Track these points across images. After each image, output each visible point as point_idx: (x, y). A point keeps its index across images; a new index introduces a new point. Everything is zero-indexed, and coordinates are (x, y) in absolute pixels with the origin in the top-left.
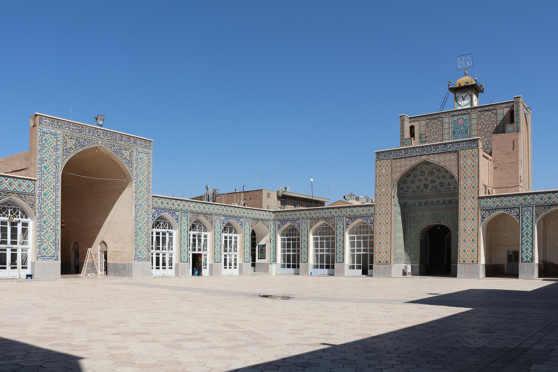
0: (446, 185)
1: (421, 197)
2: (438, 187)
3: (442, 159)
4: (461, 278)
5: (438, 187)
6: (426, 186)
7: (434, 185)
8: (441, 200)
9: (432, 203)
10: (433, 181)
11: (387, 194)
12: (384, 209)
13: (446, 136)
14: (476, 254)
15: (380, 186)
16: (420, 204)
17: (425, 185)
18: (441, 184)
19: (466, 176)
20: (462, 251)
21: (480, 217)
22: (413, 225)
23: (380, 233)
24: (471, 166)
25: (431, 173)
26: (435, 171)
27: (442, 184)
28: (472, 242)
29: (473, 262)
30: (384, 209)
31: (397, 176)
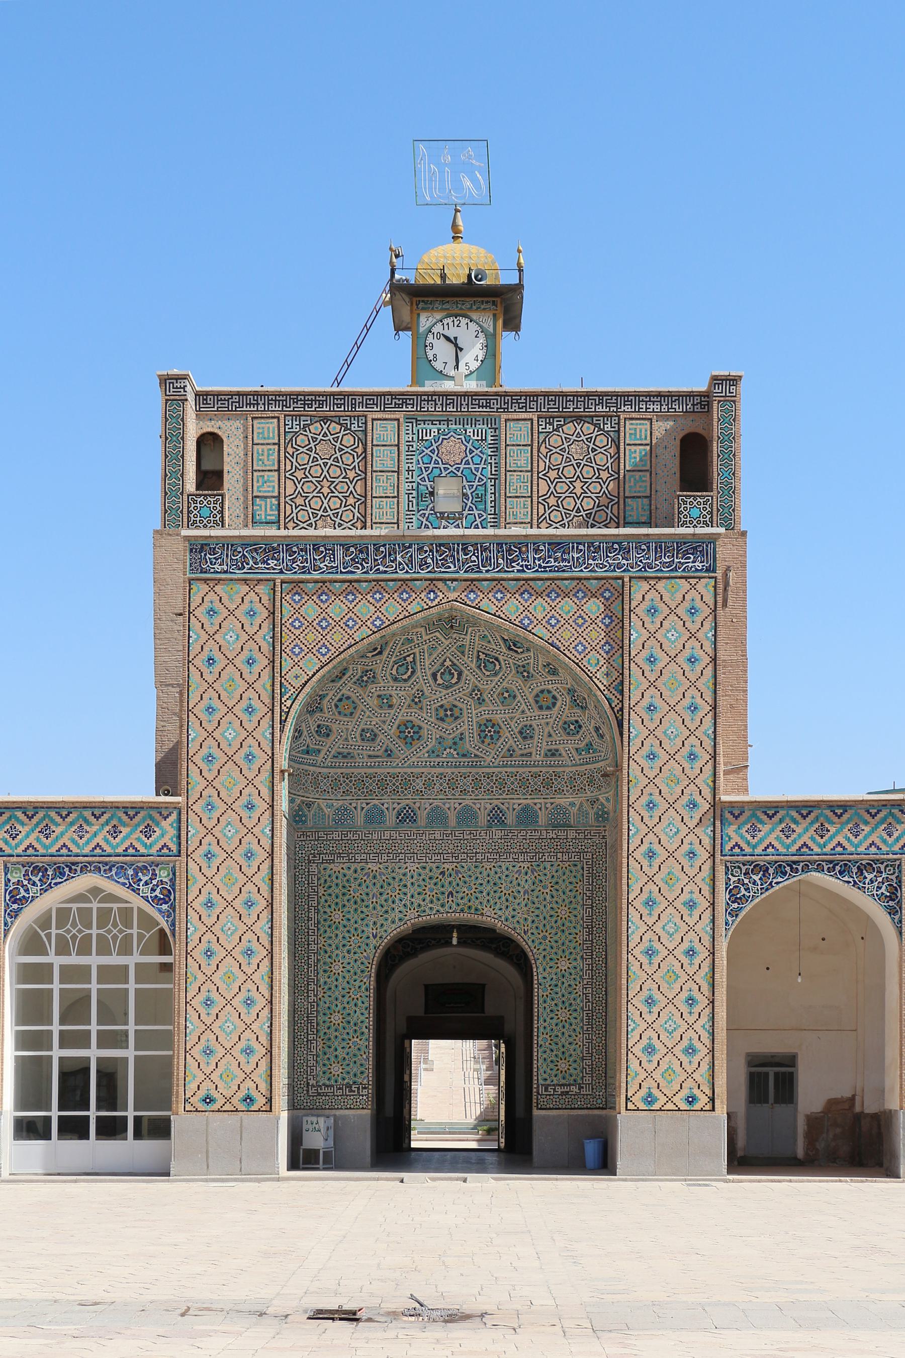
0: (508, 738)
1: (382, 784)
2: (471, 744)
3: (539, 607)
4: (641, 1175)
5: (471, 744)
8: (483, 806)
9: (437, 817)
10: (449, 713)
11: (249, 757)
12: (230, 832)
13: (382, 510)
14: (705, 1066)
15: (210, 710)
16: (374, 817)
17: (405, 724)
18: (489, 731)
19: (658, 702)
20: (638, 1050)
21: (722, 897)
22: (337, 916)
23: (209, 953)
24: (681, 659)
25: (449, 674)
26: (469, 663)
28: (684, 1008)
29: (691, 1100)
30: (230, 832)
31: (304, 669)
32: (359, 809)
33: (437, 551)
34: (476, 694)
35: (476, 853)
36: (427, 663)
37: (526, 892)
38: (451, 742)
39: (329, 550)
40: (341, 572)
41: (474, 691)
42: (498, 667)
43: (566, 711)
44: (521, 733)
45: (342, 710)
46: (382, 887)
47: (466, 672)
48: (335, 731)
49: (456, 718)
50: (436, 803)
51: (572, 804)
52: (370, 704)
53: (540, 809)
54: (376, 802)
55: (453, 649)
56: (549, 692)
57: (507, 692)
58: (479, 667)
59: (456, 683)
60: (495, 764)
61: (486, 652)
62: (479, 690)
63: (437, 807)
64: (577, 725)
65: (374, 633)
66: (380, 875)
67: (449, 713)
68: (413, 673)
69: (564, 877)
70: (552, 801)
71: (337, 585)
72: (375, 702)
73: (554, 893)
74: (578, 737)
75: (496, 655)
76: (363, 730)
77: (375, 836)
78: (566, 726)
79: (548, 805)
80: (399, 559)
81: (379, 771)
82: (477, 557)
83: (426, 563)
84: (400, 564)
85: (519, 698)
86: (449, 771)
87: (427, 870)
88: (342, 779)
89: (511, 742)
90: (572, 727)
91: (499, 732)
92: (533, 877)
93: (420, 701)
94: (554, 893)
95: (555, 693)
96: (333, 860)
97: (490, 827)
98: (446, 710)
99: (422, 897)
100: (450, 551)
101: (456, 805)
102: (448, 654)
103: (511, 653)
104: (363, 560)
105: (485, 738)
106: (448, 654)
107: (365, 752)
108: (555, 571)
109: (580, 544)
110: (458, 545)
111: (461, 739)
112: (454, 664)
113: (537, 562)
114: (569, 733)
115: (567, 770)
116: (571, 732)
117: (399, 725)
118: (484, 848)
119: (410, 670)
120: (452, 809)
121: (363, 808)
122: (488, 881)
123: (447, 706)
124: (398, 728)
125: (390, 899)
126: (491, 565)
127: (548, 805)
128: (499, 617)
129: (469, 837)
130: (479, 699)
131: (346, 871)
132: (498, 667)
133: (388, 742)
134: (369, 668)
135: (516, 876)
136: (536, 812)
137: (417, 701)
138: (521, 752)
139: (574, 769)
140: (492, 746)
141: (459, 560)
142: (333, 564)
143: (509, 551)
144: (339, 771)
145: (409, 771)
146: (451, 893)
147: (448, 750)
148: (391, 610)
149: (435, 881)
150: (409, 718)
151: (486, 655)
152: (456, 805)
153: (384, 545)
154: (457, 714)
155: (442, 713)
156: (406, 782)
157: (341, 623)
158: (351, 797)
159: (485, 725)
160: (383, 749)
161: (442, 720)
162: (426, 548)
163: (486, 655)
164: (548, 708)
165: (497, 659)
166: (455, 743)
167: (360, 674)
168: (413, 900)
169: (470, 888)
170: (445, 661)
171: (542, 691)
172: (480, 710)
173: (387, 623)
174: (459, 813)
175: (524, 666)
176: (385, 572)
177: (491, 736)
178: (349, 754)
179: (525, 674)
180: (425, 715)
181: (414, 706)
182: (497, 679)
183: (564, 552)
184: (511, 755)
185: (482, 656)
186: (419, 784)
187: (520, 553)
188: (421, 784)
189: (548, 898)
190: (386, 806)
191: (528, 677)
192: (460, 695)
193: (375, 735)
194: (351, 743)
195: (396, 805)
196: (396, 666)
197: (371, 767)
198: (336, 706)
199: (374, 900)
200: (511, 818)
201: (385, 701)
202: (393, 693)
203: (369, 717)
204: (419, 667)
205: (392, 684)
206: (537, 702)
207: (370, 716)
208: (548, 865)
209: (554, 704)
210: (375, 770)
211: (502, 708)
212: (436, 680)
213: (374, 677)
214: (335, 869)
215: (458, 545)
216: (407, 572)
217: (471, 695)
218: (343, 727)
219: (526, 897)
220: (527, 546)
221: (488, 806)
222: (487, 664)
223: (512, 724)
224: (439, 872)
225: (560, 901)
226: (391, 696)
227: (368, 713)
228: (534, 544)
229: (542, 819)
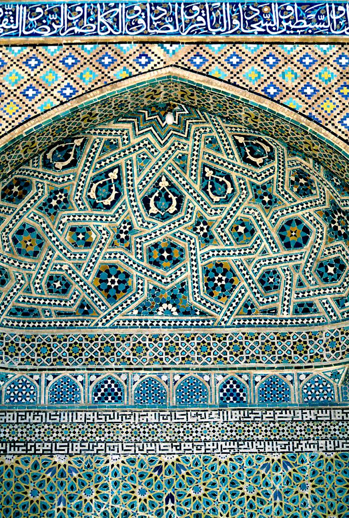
0: (246, 289)
1: (76, 350)
6: (113, 281)
7: (170, 277)
10: (166, 255)
16: (64, 393)
18: (219, 279)
26: (190, 184)
27: (220, 279)
32: (43, 383)
33: (151, 11)
34: (202, 229)
35: (205, 441)
36: (136, 182)
37: (277, 495)
38: (167, 296)
39: (8, 11)
40: (23, 35)
41: (198, 224)
42: (229, 190)
43: (323, 247)
44: (261, 281)
45: (23, 247)
46: (72, 488)
47: (188, 197)
48: (13, 277)
49: (176, 262)
50: (148, 374)
51: (336, 375)
52: (62, 239)
53: (292, 382)
54: (67, 373)
55: (170, 161)
56: (299, 222)
57: (243, 225)
58: (205, 189)
59: (175, 212)
60: (228, 324)
61: (213, 165)
62: (205, 223)
63: (151, 379)
65: (62, 103)
66: (70, 471)
67: (165, 255)
68: (118, 196)
69: (330, 473)
70: (308, 371)
71: (16, 49)
72: (68, 238)
73: (318, 495)
74: (339, 283)
75: (227, 171)
76: (51, 278)
77: (65, 419)
78: (322, 269)
79: (303, 377)
80: (101, 19)
81: (72, 332)
82: (205, 18)
83: (136, 24)
84: (102, 25)
85: (259, 233)
86: (167, 332)
87: (137, 466)
88: (20, 343)
89: (249, 293)
91: (232, 281)
92: (286, 473)
93: (127, 238)
94: (318, 495)
95: (306, 223)
96: (5, 451)
97: (223, 405)
98: (162, 251)
99: (129, 502)
100: (168, 10)
101: (177, 378)
102: (163, 170)
103: (247, 166)
104: (53, 21)
105: (214, 289)
106: (163, 170)
107: (53, 308)
108: (308, 33)
109: (340, 5)
110: (180, 4)
111: (182, 291)
112: (171, 186)
113: (284, 24)
114: (326, 280)
115: (327, 329)
116: (330, 278)
117: (100, 272)
118: (217, 434)
119: (114, 192)
120: (171, 382)
121: (48, 382)
122: (224, 480)
123: (163, 245)
124: (98, 276)
125: (84, 505)
126: (222, 26)
127: (303, 377)
128: (234, 84)
129: (194, 420)
130: (205, 235)
131: (21, 466)
132: (229, 190)
133: (84, 294)
134: (59, 187)
135: (263, 472)
136: (286, 386)
137: (123, 237)
138: (262, 308)
139: (335, 327)
140: (223, 299)
141: (180, 21)
142: (12, 26)
143: (247, 12)
144: (18, 332)
145: (112, 332)
146: (170, 497)
147: (165, 306)
148: (87, 76)
149: (147, 479)
150: (112, 261)
151: (215, 171)
152: (177, 378)
153: (82, 5)
154: (176, 255)
155: (156, 255)
156: (108, 348)
157: (18, 93)
158: (32, 367)
159: (214, 270)
160: (78, 303)
161: (156, 263)
162: (136, 8)
163: (215, 171)
164: (298, 245)
165: (228, 177)
166: (174, 297)
167: (46, 196)
168: (116, 506)
169: (197, 489)
170: (160, 180)
171: (289, 223)
172: (206, 250)
173: (81, 92)
174: (180, 387)
175: (264, 188)
176: (82, 34)
177: (222, 286)
178: (32, 310)
179: (266, 199)
180: (133, 257)
181: (119, 244)
182: (229, 206)
183: (319, 13)
184: (250, 313)
185: (209, 173)
186: (125, 349)
187: (262, 13)
188: (128, 349)
189: (309, 501)
190: (80, 378)
191: (270, 203)
192: (181, 229)
193: (68, 285)
194: (34, 295)
195: (93, 378)
196: (95, 186)
197: (60, 327)
198: (15, 241)
199: (61, 506)
200: (252, 395)
201: (81, 236)
202: (91, 225)
203: (59, 258)
204: (125, 188)
205: (90, 210)
206: (282, 238)
207: (60, 258)
208: (307, 457)
209: (305, 240)
210: (66, 331)
211: (235, 246)
212: (148, 208)
213: (66, 201)
214: (7, 463)
215: (180, 4)
216: (111, 34)
217: (195, 229)
218: (25, 272)
219: (278, 501)
220: (270, 6)
221: (220, 378)
222: (216, 184)
223: (250, 269)
224: (154, 467)
225: (326, 506)
226: (88, 229)
227: (57, 253)
228: (279, 4)
229: (295, 396)
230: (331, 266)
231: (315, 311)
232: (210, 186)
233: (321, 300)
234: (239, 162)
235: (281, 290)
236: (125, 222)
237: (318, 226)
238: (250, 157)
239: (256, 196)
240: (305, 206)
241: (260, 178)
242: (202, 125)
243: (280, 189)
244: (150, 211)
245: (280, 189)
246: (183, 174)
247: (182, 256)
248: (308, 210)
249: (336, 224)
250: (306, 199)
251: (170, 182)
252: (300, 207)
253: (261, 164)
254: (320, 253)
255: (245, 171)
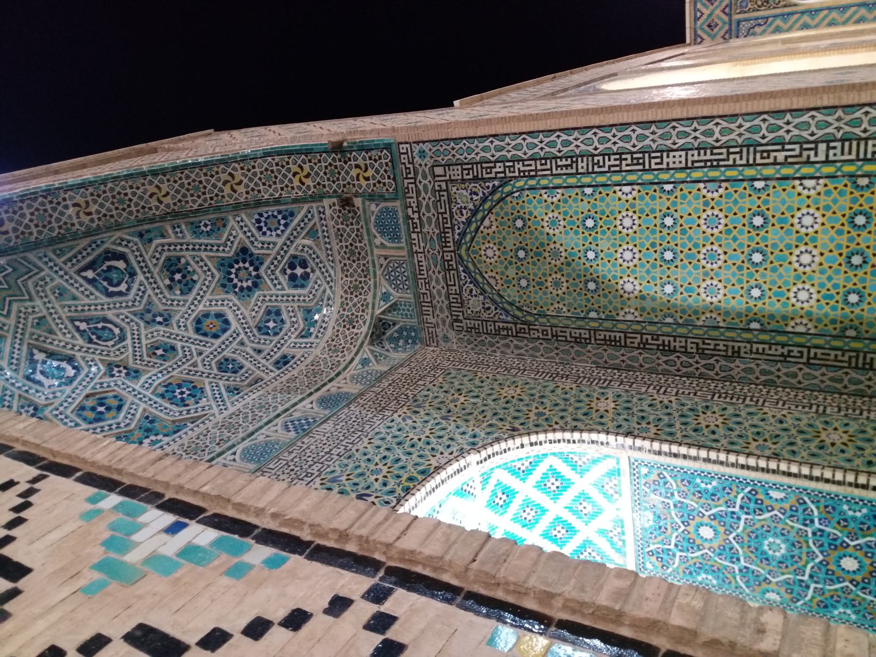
34: (120, 372)
41: (112, 370)
42: (117, 331)
43: (247, 313)
49: (119, 408)
51: (365, 362)
56: (207, 315)
57: (158, 348)
58: (90, 341)
64: (273, 316)
74: (287, 325)
75: (100, 313)
90: (271, 324)
95: (214, 309)
103: (115, 299)
114: (276, 334)
116: (277, 330)
130: (127, 374)
154: (114, 403)
163: (87, 321)
164: (224, 331)
165: (105, 320)
166: (148, 430)
171: (198, 321)
179: (159, 319)
182: (129, 341)
185: (83, 326)
191: (165, 320)
206: (205, 335)
209: (227, 322)
230: (268, 321)
231: (293, 357)
232: (94, 337)
233: (289, 347)
234: (105, 299)
235: (247, 364)
236: (23, 407)
237: (226, 303)
238: (111, 289)
239: (148, 323)
240: (199, 298)
241: (137, 303)
242: (38, 276)
243: (164, 301)
244: (46, 385)
245: (164, 301)
246: (54, 337)
247: (121, 400)
248: (205, 299)
249: (239, 284)
250: (195, 292)
251: (45, 352)
252: (196, 302)
253: (128, 289)
254: (249, 320)
255: (118, 305)
